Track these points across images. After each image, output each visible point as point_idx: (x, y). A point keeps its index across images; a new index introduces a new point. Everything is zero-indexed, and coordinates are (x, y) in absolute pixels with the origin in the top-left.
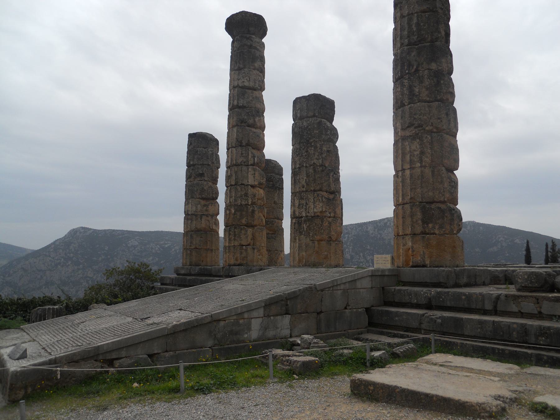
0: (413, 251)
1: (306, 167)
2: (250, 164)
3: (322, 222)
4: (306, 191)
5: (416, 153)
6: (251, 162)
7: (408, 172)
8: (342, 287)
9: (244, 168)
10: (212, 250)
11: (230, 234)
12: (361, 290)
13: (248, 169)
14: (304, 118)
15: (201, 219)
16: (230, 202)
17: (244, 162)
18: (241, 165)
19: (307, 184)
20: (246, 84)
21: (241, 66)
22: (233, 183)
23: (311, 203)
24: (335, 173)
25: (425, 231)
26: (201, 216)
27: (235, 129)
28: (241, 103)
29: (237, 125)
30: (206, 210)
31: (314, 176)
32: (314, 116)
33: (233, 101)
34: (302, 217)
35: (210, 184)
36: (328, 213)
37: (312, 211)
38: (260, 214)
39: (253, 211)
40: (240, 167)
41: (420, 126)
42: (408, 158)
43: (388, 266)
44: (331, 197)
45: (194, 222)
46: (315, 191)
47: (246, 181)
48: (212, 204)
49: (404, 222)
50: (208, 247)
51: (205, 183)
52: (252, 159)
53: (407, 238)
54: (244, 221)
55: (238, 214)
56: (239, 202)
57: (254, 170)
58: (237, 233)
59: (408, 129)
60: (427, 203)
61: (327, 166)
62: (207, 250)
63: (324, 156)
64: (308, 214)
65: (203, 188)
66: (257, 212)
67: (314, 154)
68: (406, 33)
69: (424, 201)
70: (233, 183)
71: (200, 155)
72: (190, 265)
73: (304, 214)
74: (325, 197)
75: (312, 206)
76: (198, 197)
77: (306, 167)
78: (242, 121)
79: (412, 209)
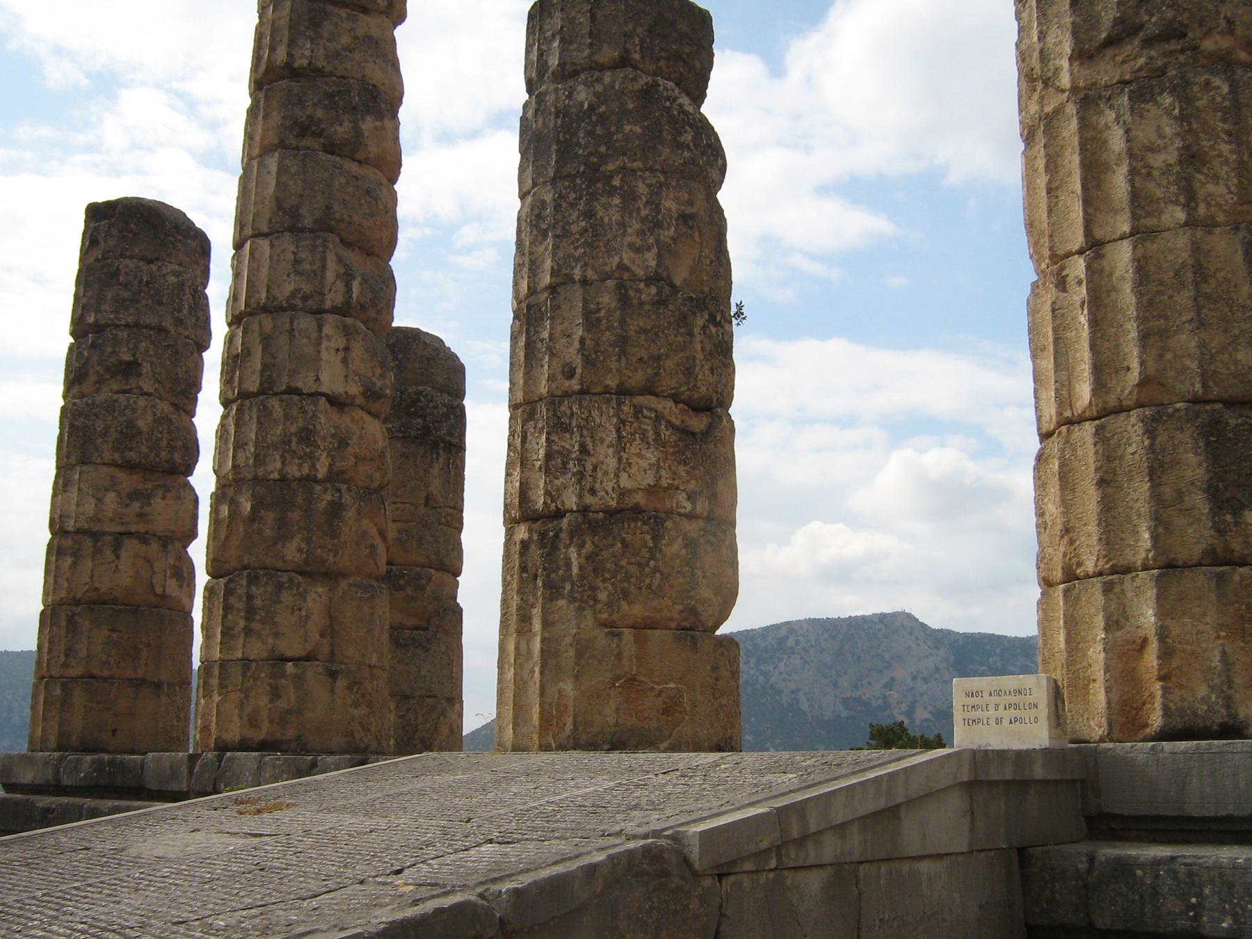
0: (1166, 654)
1: (585, 282)
2: (328, 305)
3: (657, 537)
4: (583, 392)
5: (1157, 161)
6: (334, 297)
7: (1122, 257)
8: (830, 849)
9: (305, 322)
10: (158, 686)
11: (227, 608)
12: (924, 867)
13: (320, 327)
14: (576, 73)
16: (235, 467)
17: (305, 298)
18: (292, 308)
19: (589, 362)
22: (253, 386)
23: (602, 450)
24: (712, 319)
25: (1227, 549)
26: (119, 539)
28: (305, 54)
29: (282, 145)
30: (141, 516)
31: (623, 322)
32: (624, 62)
33: (272, 49)
34: (559, 514)
35: (164, 407)
36: (682, 497)
37: (609, 486)
38: (366, 524)
39: (336, 510)
40: (285, 318)
42: (1119, 183)
43: (1035, 734)
44: (698, 423)
46: (623, 392)
47: (312, 375)
48: (167, 489)
50: (141, 672)
51: (142, 402)
52: (340, 286)
54: (292, 551)
56: (274, 467)
57: (348, 332)
58: (258, 602)
59: (1109, 52)
60: (1230, 403)
61: (678, 281)
62: (137, 683)
63: (667, 234)
64: (589, 500)
65: (131, 424)
66: (350, 514)
67: (623, 225)
69: (1215, 392)
70: (253, 385)
71: (126, 286)
72: (60, 748)
73: (570, 500)
74: (669, 423)
75: (612, 463)
76: (107, 457)
77: (585, 282)
78: (305, 129)
79: (1150, 433)
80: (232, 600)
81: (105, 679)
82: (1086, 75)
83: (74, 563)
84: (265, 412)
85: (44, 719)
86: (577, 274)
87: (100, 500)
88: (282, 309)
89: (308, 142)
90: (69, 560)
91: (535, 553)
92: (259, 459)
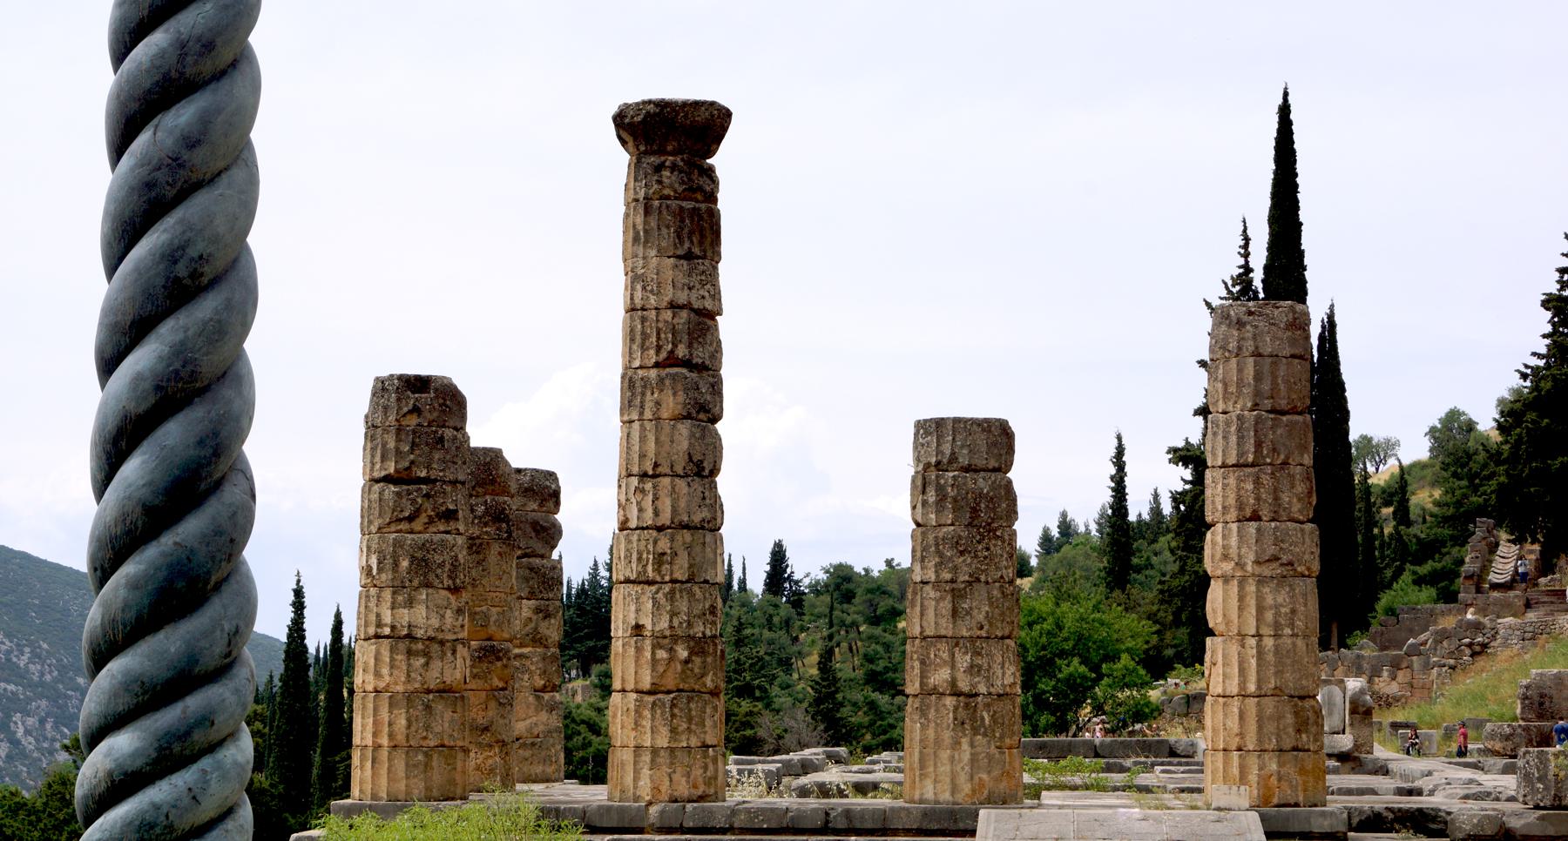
0: (1279, 780)
7: (1269, 642)
11: (673, 716)
15: (454, 652)
19: (991, 624)
20: (708, 304)
21: (696, 250)
22: (678, 575)
27: (684, 428)
29: (688, 417)
34: (977, 695)
41: (1291, 564)
45: (436, 665)
46: (1003, 638)
49: (1260, 728)
53: (1266, 756)
55: (697, 660)
56: (699, 629)
68: (1266, 387)
73: (982, 689)
75: (999, 672)
80: (676, 711)
81: (451, 748)
82: (1258, 570)
83: (427, 664)
84: (691, 594)
85: (407, 778)
86: (983, 578)
87: (443, 616)
88: (696, 528)
89: (702, 416)
90: (422, 661)
91: (962, 713)
92: (690, 625)
